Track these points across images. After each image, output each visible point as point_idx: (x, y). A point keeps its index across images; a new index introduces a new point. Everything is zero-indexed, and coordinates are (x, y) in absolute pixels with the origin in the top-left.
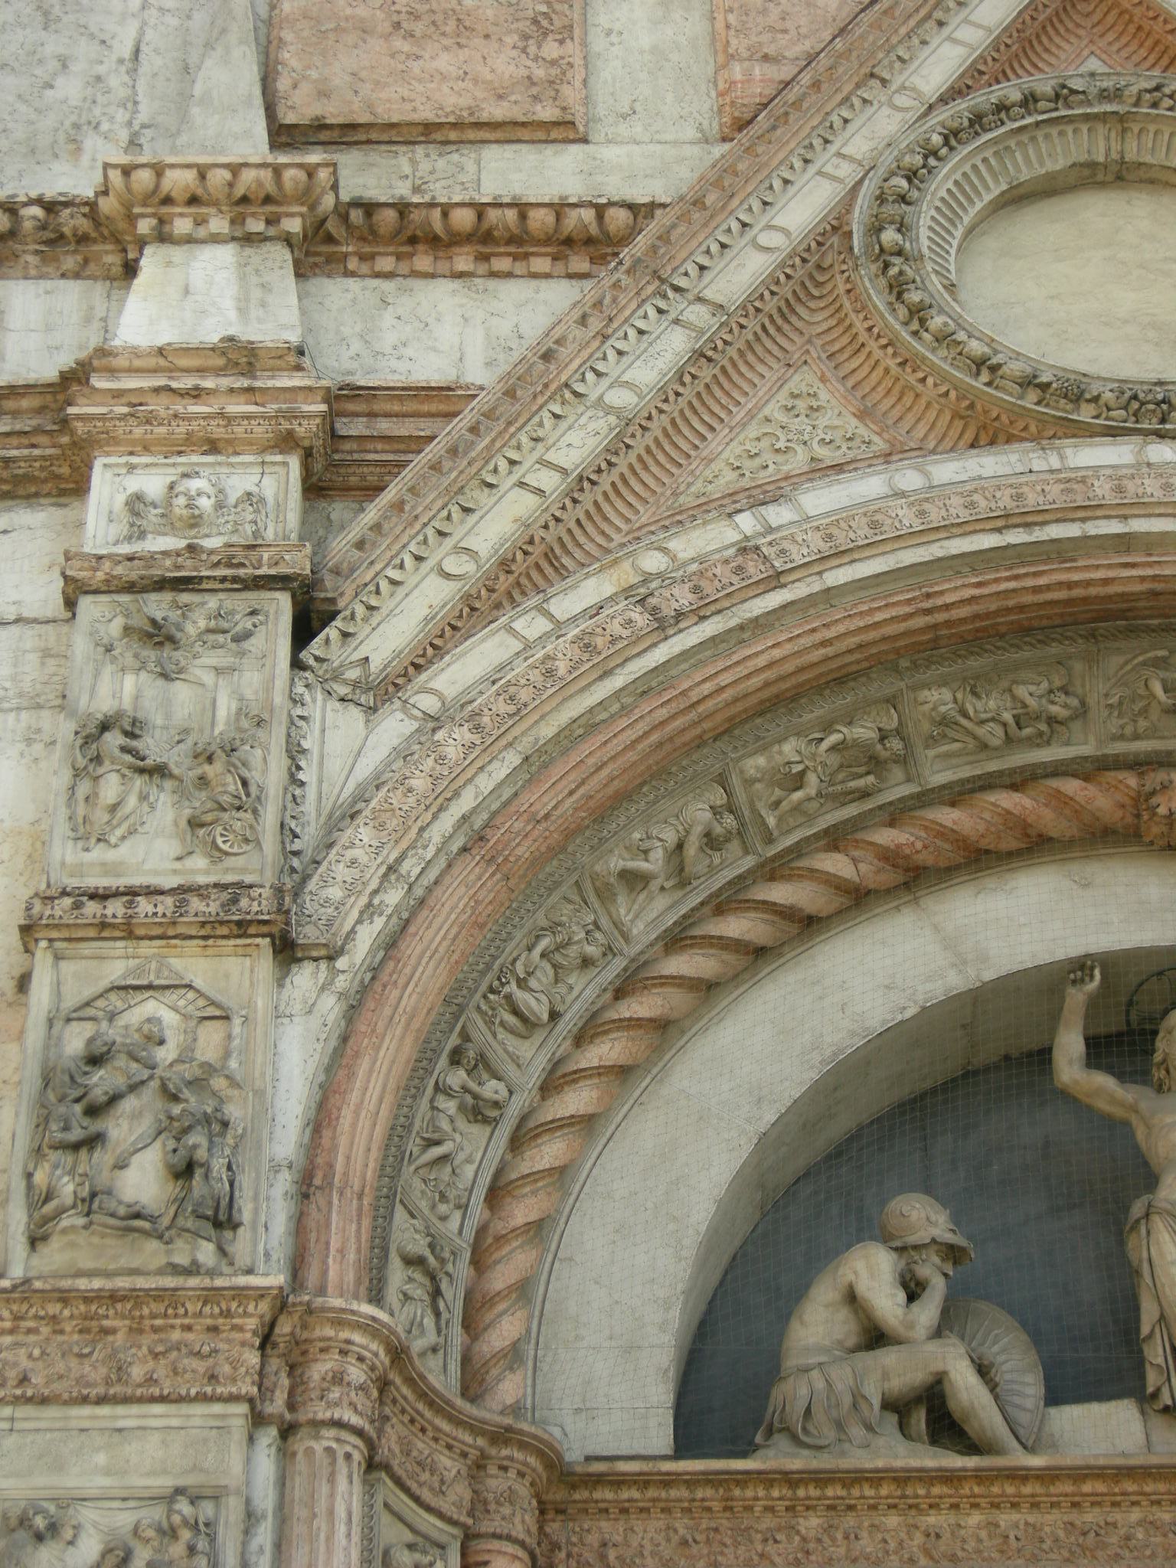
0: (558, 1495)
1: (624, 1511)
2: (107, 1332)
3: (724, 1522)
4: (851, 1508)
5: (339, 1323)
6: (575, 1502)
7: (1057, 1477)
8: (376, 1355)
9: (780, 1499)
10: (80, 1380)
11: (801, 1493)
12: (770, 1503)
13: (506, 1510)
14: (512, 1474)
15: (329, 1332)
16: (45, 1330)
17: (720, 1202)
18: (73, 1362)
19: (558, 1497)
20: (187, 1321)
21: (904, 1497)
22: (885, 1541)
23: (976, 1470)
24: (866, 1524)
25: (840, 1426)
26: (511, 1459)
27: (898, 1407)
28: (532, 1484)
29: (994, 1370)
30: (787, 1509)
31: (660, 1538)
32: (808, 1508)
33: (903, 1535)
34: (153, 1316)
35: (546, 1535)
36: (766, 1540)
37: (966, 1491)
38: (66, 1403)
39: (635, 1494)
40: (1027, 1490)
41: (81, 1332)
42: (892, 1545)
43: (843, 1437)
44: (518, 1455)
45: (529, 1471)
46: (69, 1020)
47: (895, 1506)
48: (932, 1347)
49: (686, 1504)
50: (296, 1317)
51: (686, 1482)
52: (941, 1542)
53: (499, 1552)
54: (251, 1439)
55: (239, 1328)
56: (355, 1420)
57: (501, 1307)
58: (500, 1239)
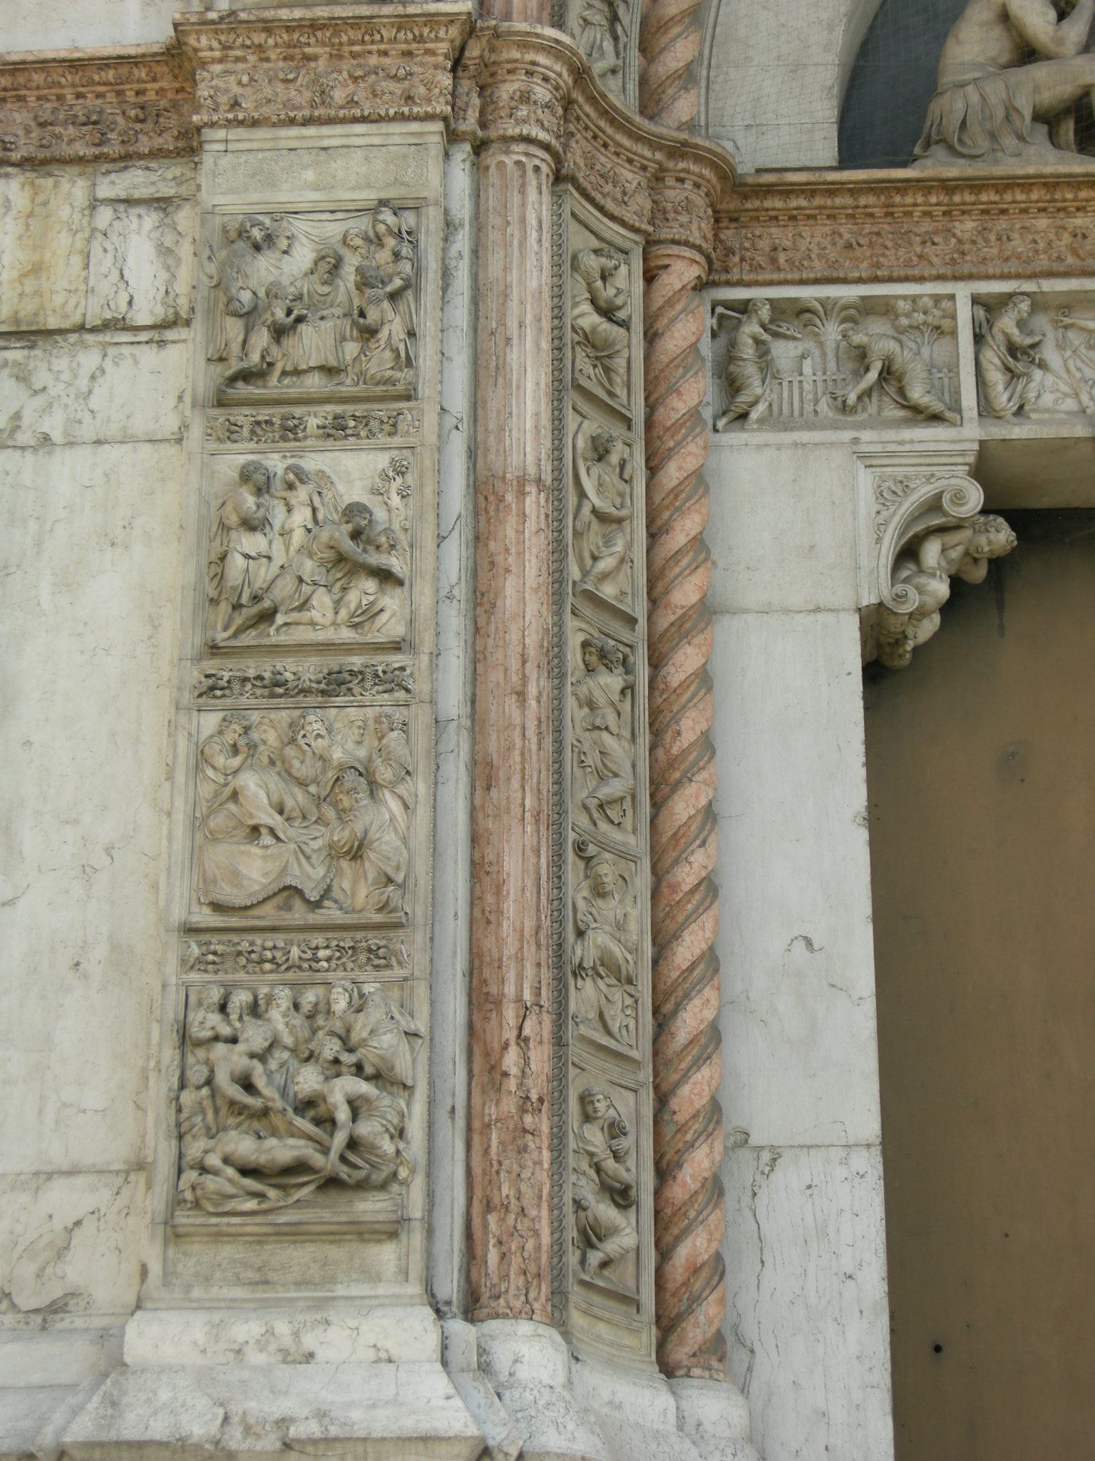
0: (731, 204)
1: (793, 218)
2: (308, 58)
3: (886, 226)
4: (1003, 212)
5: (524, 46)
6: (747, 210)
8: (560, 75)
9: (937, 205)
12: (928, 208)
13: (684, 218)
14: (688, 185)
15: (516, 54)
16: (252, 59)
18: (280, 87)
19: (731, 206)
20: (382, 47)
22: (1035, 242)
24: (1018, 226)
25: (993, 136)
26: (687, 171)
27: (1048, 119)
28: (707, 195)
30: (944, 213)
31: (826, 243)
32: (963, 213)
33: (1051, 236)
34: (352, 43)
35: (721, 241)
36: (924, 243)
38: (274, 125)
41: (285, 59)
42: (1042, 245)
43: (996, 147)
44: (694, 168)
45: (704, 182)
47: (1044, 210)
48: (1081, 61)
49: (850, 211)
50: (484, 40)
51: (850, 190)
52: (1087, 242)
53: (678, 256)
54: (447, 155)
55: (432, 53)
56: (543, 136)
57: (676, 30)
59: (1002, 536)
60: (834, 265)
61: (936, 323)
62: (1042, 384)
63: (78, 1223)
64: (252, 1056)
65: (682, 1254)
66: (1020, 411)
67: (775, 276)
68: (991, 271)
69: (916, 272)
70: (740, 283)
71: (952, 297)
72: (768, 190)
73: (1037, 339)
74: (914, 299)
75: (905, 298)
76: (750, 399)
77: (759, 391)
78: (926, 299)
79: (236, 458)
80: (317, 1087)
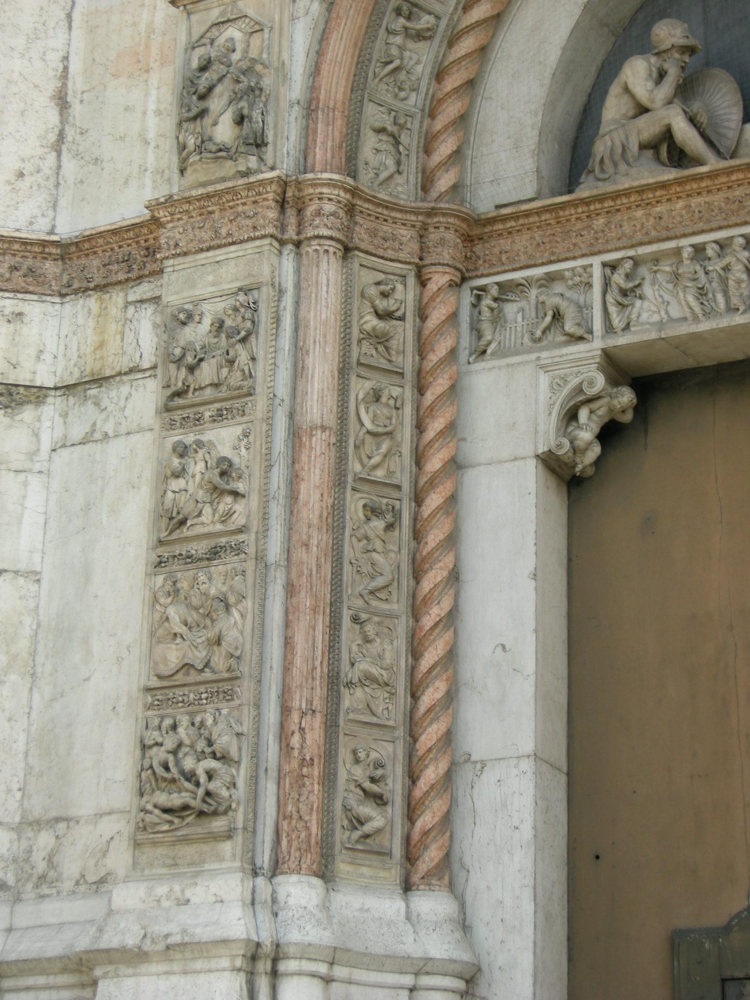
0: (476, 231)
1: (510, 233)
2: (211, 213)
3: (558, 229)
4: (618, 210)
5: (314, 185)
7: (718, 175)
8: (338, 195)
10: (201, 241)
11: (592, 208)
14: (442, 229)
15: (311, 191)
16: (185, 218)
17: (564, 49)
18: (197, 231)
19: (477, 232)
20: (243, 201)
21: (642, 200)
22: (635, 226)
23: (675, 179)
25: (615, 165)
26: (440, 222)
27: (651, 146)
28: (456, 231)
29: (698, 116)
30: (588, 217)
31: (528, 244)
33: (644, 220)
34: (228, 201)
35: (474, 252)
37: (673, 191)
38: (194, 253)
39: (513, 223)
40: (703, 184)
41: (200, 215)
42: (639, 226)
46: (194, 48)
50: (293, 187)
52: (662, 221)
53: (436, 272)
54: (280, 252)
55: (265, 199)
57: (442, 138)
58: (441, 101)
59: (626, 397)
60: (531, 257)
61: (586, 281)
62: (641, 308)
63: (112, 838)
64: (169, 752)
65: (419, 824)
66: (627, 327)
67: (499, 269)
68: (610, 248)
69: (571, 255)
70: (482, 276)
71: (591, 265)
72: (493, 221)
73: (637, 282)
74: (573, 269)
75: (568, 270)
76: (485, 343)
77: (489, 338)
78: (578, 269)
79: (176, 437)
80: (192, 766)
